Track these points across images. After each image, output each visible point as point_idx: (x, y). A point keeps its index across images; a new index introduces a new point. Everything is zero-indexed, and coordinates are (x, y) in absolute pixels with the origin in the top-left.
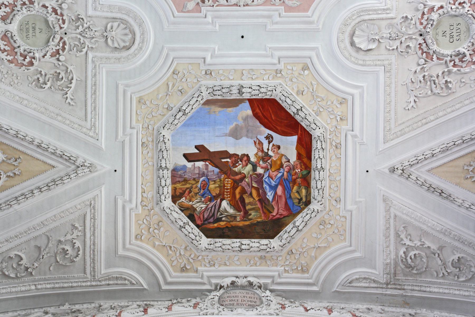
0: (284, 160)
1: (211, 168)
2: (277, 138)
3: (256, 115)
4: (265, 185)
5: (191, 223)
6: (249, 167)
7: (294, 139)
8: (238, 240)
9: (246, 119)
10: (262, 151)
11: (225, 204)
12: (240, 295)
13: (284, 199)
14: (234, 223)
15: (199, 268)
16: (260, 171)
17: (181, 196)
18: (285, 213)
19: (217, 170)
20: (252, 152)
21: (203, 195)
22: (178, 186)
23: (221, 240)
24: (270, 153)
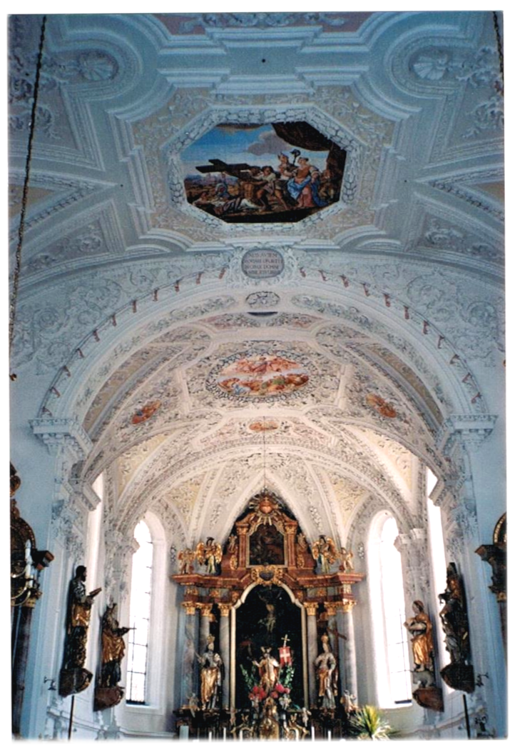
0: (311, 170)
1: (228, 176)
2: (305, 153)
3: (280, 134)
4: (289, 188)
6: (272, 176)
7: (326, 153)
9: (267, 139)
10: (288, 162)
11: (245, 201)
12: (263, 258)
13: (310, 197)
14: (257, 213)
15: (221, 240)
16: (283, 178)
17: (197, 197)
18: (312, 206)
19: (235, 178)
20: (275, 164)
21: (221, 196)
22: (193, 191)
24: (296, 164)
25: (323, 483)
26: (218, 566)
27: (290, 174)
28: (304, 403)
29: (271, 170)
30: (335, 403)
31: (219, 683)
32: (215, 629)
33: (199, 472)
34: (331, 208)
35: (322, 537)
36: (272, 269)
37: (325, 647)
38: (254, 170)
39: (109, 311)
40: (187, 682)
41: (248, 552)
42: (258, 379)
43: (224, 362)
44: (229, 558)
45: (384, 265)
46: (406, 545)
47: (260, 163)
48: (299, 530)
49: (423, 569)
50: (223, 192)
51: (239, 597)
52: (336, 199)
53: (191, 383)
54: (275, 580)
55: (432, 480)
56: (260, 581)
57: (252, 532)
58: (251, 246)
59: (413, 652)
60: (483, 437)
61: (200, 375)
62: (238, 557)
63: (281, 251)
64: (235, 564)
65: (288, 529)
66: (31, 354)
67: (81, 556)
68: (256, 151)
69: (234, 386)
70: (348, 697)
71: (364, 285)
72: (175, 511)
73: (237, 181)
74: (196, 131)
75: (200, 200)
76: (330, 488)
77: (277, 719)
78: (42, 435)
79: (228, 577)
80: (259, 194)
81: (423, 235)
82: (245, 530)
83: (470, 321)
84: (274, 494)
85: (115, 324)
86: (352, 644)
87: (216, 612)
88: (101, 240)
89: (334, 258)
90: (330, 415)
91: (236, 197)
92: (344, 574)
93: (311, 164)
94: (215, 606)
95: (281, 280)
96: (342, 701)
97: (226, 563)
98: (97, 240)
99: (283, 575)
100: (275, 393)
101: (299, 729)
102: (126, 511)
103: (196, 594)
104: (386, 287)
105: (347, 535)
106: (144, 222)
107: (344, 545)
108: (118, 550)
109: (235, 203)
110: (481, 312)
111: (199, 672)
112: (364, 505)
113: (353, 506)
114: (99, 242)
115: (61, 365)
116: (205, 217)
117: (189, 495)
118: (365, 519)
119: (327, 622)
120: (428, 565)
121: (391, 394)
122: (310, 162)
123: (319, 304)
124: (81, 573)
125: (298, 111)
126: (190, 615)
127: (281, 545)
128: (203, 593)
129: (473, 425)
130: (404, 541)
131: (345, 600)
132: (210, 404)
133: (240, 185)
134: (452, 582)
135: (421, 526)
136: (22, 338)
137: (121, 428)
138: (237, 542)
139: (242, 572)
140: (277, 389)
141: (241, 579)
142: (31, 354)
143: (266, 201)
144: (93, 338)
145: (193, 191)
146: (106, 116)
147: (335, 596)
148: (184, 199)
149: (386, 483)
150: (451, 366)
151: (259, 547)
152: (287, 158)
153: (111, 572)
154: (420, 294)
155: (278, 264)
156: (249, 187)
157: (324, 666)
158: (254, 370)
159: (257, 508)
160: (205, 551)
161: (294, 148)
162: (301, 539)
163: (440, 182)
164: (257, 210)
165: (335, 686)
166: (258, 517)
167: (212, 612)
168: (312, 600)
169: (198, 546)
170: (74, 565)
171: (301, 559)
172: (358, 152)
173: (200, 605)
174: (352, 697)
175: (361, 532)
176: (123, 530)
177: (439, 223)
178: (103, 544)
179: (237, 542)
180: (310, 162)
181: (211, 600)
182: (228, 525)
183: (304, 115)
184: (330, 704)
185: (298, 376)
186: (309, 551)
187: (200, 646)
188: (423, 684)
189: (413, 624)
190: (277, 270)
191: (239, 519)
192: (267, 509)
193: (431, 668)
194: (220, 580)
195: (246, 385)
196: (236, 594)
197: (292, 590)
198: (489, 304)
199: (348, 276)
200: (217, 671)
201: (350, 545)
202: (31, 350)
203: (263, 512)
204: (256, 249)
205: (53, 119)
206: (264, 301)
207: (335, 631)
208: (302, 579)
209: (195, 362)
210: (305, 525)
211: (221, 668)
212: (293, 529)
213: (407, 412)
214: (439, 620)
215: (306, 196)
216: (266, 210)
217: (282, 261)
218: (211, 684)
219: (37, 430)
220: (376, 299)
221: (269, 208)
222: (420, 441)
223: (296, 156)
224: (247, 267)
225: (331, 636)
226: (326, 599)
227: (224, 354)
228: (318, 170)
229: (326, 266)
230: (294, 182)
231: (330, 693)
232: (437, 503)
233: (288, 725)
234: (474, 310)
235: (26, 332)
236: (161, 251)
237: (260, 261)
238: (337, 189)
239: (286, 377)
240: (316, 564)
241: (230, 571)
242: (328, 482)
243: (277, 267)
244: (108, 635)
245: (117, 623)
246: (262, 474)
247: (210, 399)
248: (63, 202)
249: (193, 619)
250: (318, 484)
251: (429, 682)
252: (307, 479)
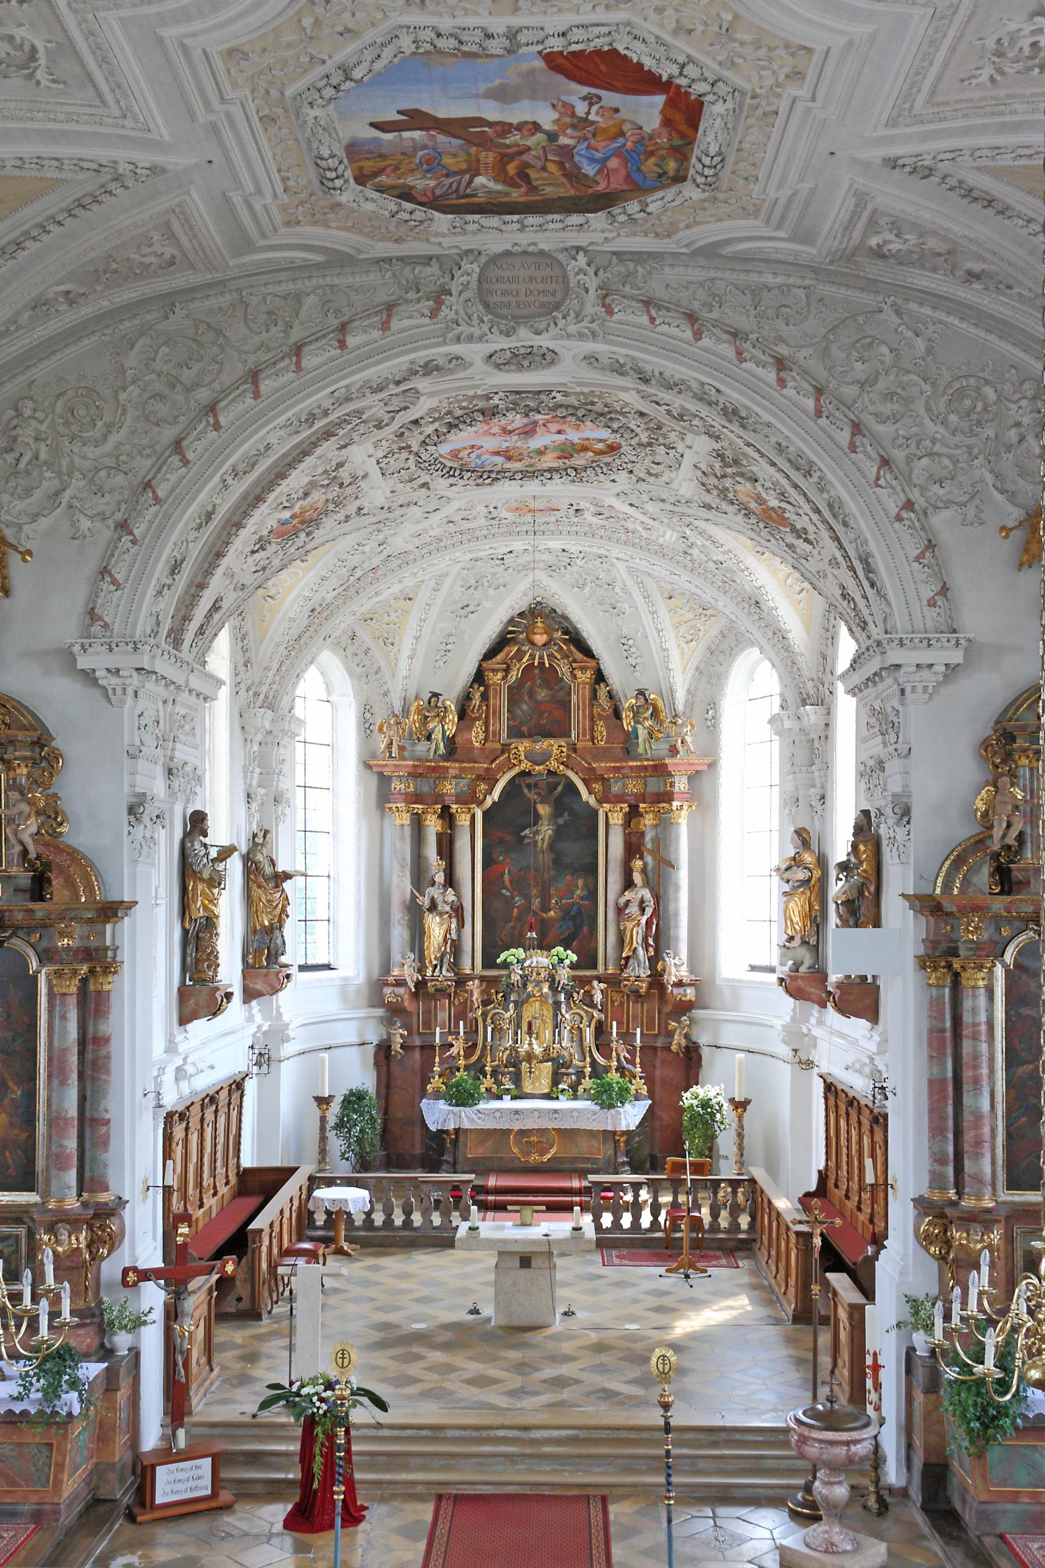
0: (626, 127)
1: (441, 138)
2: (610, 98)
4: (577, 158)
5: (408, 206)
6: (539, 137)
8: (516, 217)
10: (573, 115)
11: (480, 180)
16: (563, 140)
18: (626, 187)
20: (547, 118)
21: (428, 171)
22: (366, 164)
23: (477, 217)
25: (647, 597)
26: (450, 742)
27: (576, 134)
28: (614, 481)
29: (536, 127)
30: (674, 486)
31: (454, 937)
32: (447, 848)
33: (410, 582)
34: (670, 193)
35: (641, 693)
36: (542, 298)
37: (637, 878)
38: (499, 128)
39: (203, 395)
40: (399, 934)
41: (505, 715)
42: (519, 444)
43: (451, 426)
44: (470, 728)
45: (780, 287)
46: (790, 730)
47: (517, 113)
48: (600, 677)
49: (816, 773)
50: (431, 164)
51: (490, 792)
52: (680, 178)
53: (386, 461)
54: (553, 765)
55: (847, 647)
56: (526, 765)
57: (514, 675)
58: (498, 248)
59: (787, 918)
60: (941, 678)
61: (401, 448)
62: (487, 724)
63: (561, 257)
64: (482, 736)
65: (578, 673)
66: (57, 494)
67: (198, 789)
68: (503, 95)
69: (473, 456)
70: (670, 961)
71: (735, 335)
72: (369, 642)
73: (461, 146)
74: (365, 65)
75: (383, 178)
76: (662, 606)
77: (550, 1001)
78: (94, 671)
79: (469, 762)
80: (512, 169)
81: (862, 241)
82: (500, 675)
83: (944, 423)
84: (555, 611)
85: (217, 426)
86: (683, 876)
87: (447, 816)
88: (175, 252)
89: (676, 270)
90: (663, 501)
91: (462, 173)
92: (677, 760)
93: (625, 117)
94: (446, 809)
95: (561, 323)
96: (659, 967)
97: (466, 736)
98: (167, 256)
99: (568, 756)
100: (555, 464)
101: (586, 1012)
102: (275, 666)
103: (412, 789)
104: (781, 339)
105: (686, 687)
106: (264, 220)
107: (680, 707)
108: (265, 737)
109: (459, 183)
110: (968, 402)
111: (422, 918)
112: (722, 633)
113: (701, 634)
114: (173, 257)
115: (119, 516)
116: (395, 208)
117: (393, 616)
118: (721, 658)
119: (642, 834)
120: (827, 767)
121: (782, 494)
122: (623, 114)
123: (639, 371)
124: (197, 822)
125: (597, 30)
126: (402, 825)
127: (565, 705)
128: (425, 788)
129: (925, 656)
130: (787, 724)
131: (675, 804)
132: (425, 485)
133: (468, 154)
134: (862, 848)
135: (820, 702)
136: (36, 457)
137: (253, 552)
138: (485, 697)
139: (494, 750)
140: (559, 458)
141: (492, 762)
142: (57, 494)
143: (526, 179)
144: (175, 460)
145: (366, 164)
146: (160, 41)
147: (657, 794)
148: (346, 181)
149: (764, 615)
150: (897, 525)
151: (525, 707)
152: (573, 107)
153: (256, 776)
154: (848, 355)
155: (555, 286)
156: (489, 157)
157: (634, 909)
158: (511, 432)
159: (523, 636)
160: (426, 717)
161: (586, 90)
162: (602, 691)
163: (907, 161)
164: (507, 194)
165: (651, 941)
166: (525, 653)
167: (441, 817)
168: (619, 799)
169: (413, 708)
170: (186, 808)
171: (601, 729)
172: (730, 105)
173: (419, 807)
174: (677, 961)
175: (713, 681)
176: (270, 704)
177: (897, 227)
178: (238, 730)
179: (485, 697)
180: (623, 114)
181: (438, 798)
182: (469, 668)
183: (608, 39)
184: (640, 971)
185: (600, 441)
186: (617, 714)
187: (420, 877)
188: (796, 968)
189: (787, 869)
190: (550, 298)
191: (491, 654)
192: (540, 639)
193: (813, 941)
194: (453, 768)
195: (497, 453)
196: (483, 787)
197: (584, 780)
198: (987, 382)
199: (704, 314)
200: (450, 917)
201: (690, 704)
202: (56, 484)
203: (533, 643)
204: (507, 253)
205: (41, 54)
206: (526, 363)
207: (655, 852)
208: (600, 766)
209: (388, 432)
210: (609, 667)
211: (458, 911)
212: (588, 674)
213: (811, 529)
214: (832, 908)
215: (615, 170)
216: (527, 194)
217: (565, 278)
218: (441, 939)
219: (84, 662)
220: (760, 371)
221: (533, 189)
222: (830, 576)
223: (591, 105)
224: (489, 292)
225: (649, 859)
226: (642, 797)
227: (448, 413)
228: (641, 128)
229: (658, 290)
230: (588, 147)
231: (641, 952)
232: (852, 691)
233: (569, 1008)
234: (960, 394)
235: (43, 445)
236: (305, 260)
237: (514, 280)
238: (682, 153)
239: (576, 441)
240: (630, 738)
241: (473, 748)
242: (656, 595)
243: (554, 294)
244: (260, 886)
245: (273, 863)
246: (530, 578)
247: (425, 478)
248: (87, 200)
249: (408, 831)
250: (639, 600)
251: (808, 962)
252: (617, 590)
